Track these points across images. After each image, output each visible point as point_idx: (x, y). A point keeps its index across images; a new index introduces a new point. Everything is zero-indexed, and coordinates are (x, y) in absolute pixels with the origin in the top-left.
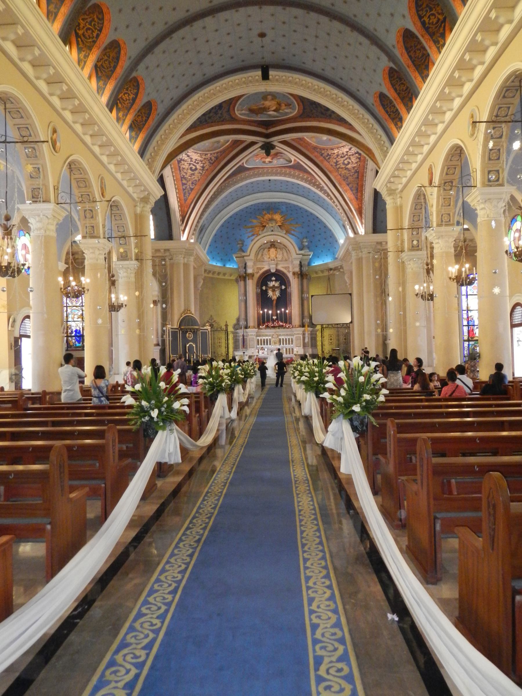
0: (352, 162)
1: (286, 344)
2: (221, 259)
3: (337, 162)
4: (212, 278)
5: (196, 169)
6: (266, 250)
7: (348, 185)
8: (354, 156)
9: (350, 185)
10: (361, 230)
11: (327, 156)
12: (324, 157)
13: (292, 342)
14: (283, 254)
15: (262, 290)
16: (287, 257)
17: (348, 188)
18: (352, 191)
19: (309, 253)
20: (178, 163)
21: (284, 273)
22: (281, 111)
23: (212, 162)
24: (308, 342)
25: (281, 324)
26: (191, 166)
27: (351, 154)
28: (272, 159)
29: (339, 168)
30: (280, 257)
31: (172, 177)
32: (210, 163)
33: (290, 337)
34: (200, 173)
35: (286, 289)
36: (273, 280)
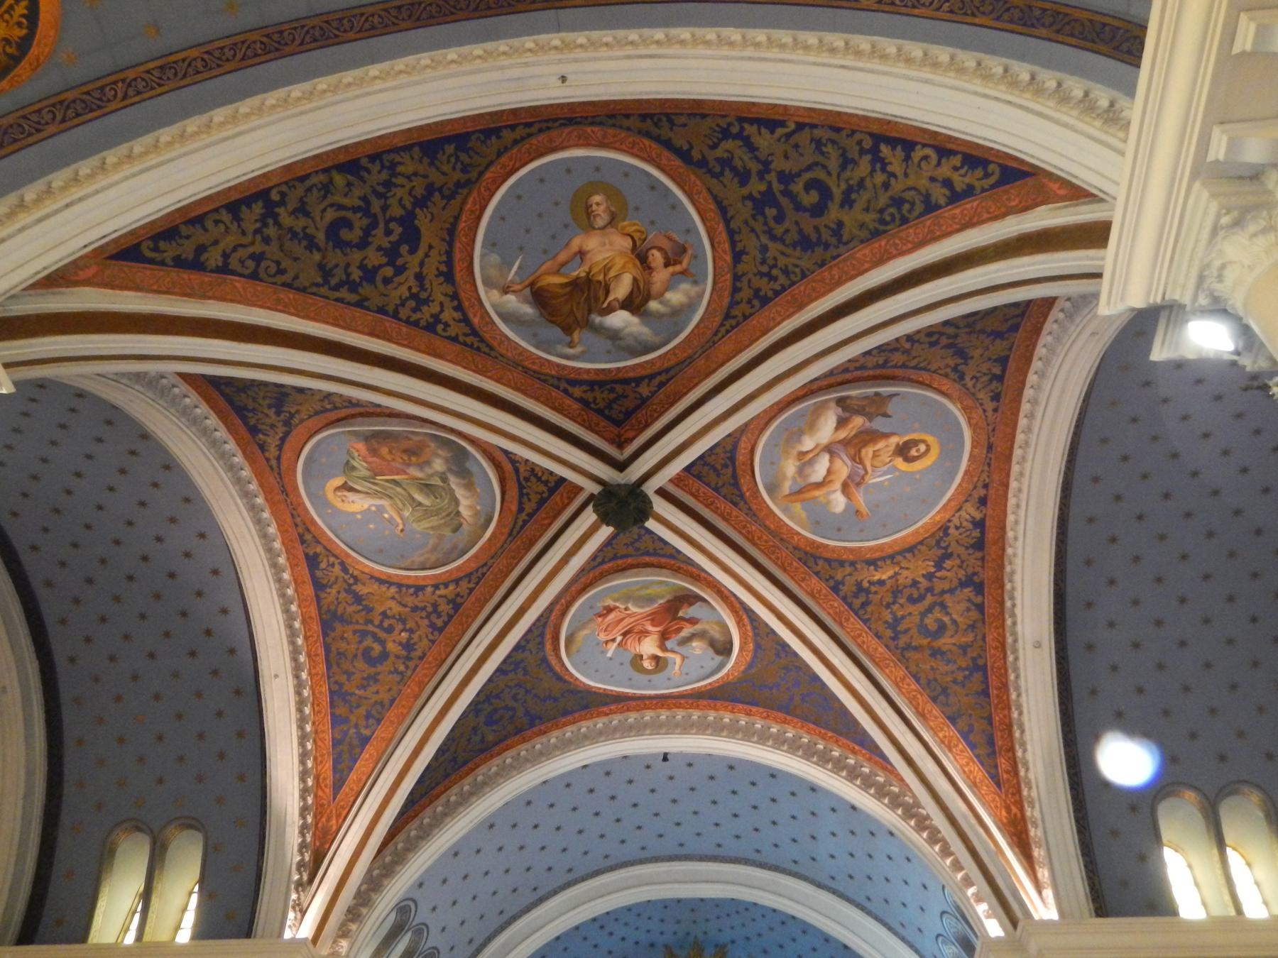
0: (955, 622)
3: (897, 621)
5: (384, 655)
7: (953, 720)
8: (958, 592)
9: (962, 722)
10: (1043, 908)
11: (856, 596)
12: (844, 599)
17: (951, 732)
18: (972, 746)
20: (325, 635)
22: (653, 305)
23: (439, 623)
26: (368, 642)
27: (947, 587)
28: (663, 647)
29: (908, 647)
31: (291, 682)
32: (433, 626)
34: (396, 671)
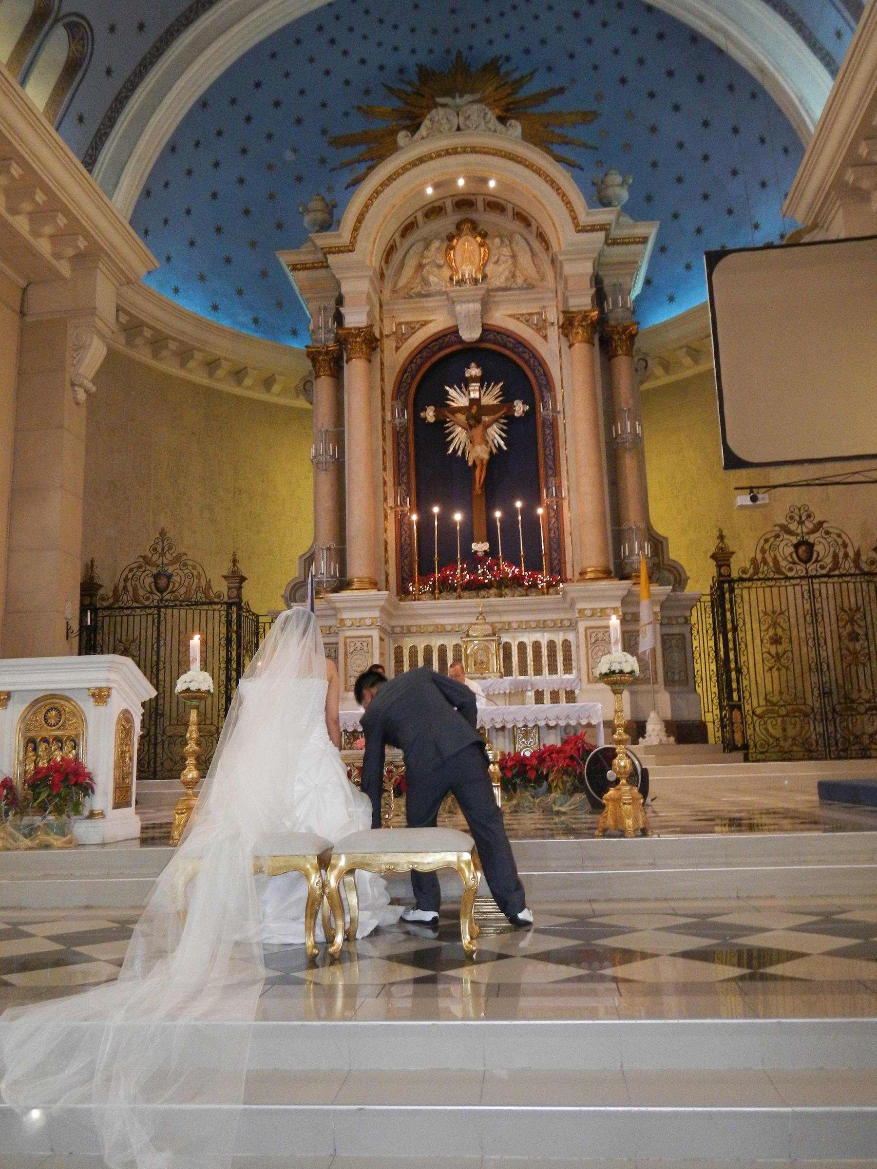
1: (538, 671)
2: (256, 321)
4: (209, 392)
6: (436, 244)
13: (568, 659)
14: (514, 256)
15: (418, 421)
16: (532, 271)
19: (640, 230)
21: (520, 344)
24: (654, 650)
25: (511, 571)
30: (499, 274)
33: (559, 638)
35: (531, 415)
36: (474, 379)
